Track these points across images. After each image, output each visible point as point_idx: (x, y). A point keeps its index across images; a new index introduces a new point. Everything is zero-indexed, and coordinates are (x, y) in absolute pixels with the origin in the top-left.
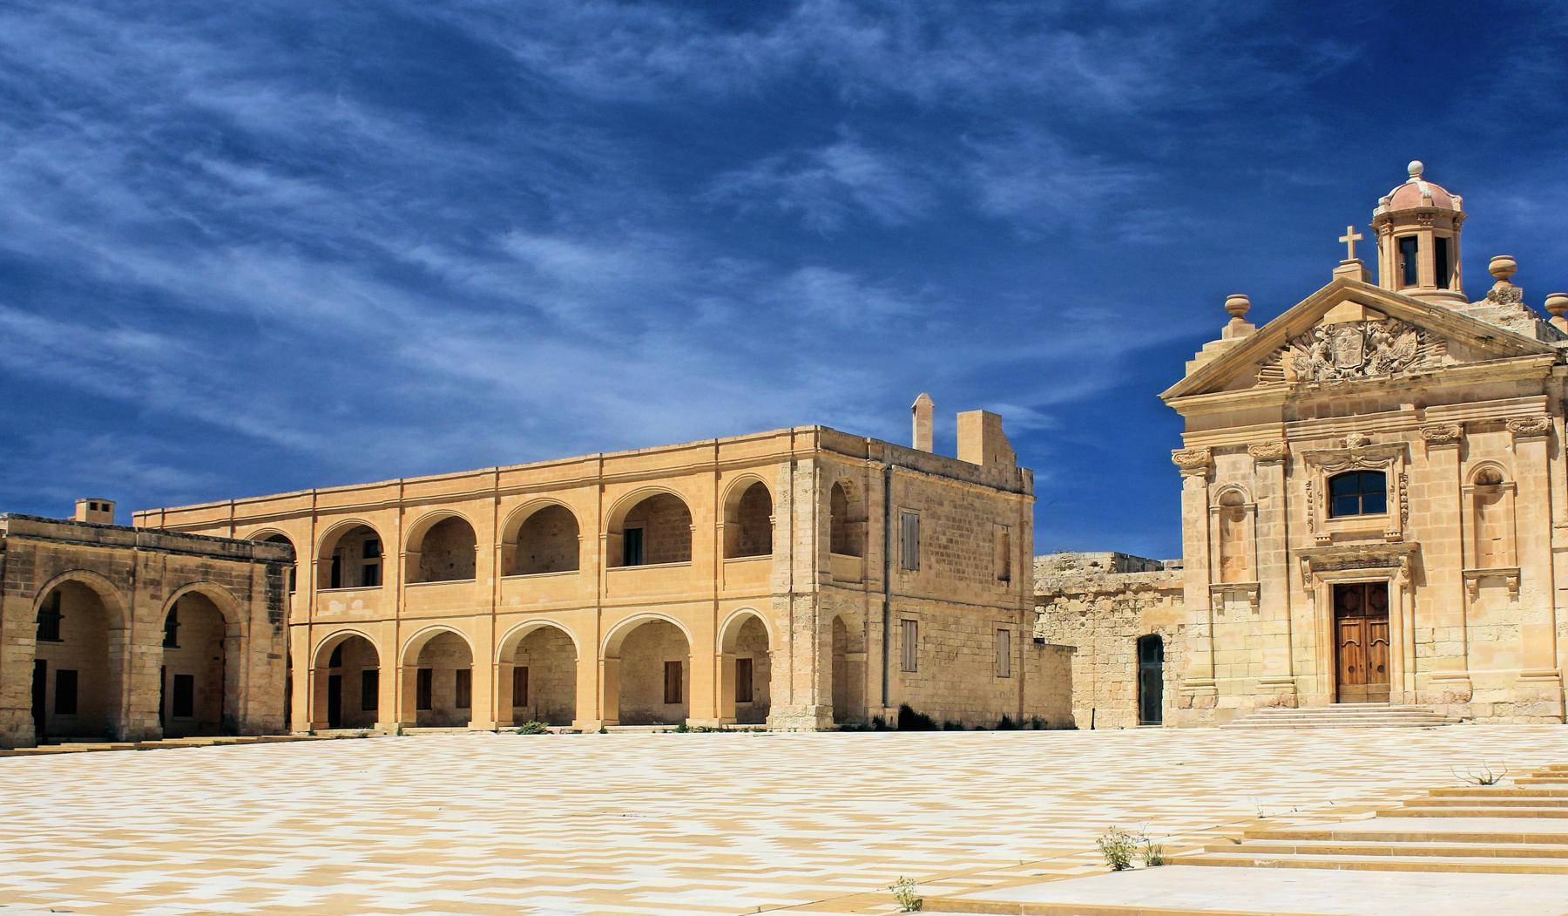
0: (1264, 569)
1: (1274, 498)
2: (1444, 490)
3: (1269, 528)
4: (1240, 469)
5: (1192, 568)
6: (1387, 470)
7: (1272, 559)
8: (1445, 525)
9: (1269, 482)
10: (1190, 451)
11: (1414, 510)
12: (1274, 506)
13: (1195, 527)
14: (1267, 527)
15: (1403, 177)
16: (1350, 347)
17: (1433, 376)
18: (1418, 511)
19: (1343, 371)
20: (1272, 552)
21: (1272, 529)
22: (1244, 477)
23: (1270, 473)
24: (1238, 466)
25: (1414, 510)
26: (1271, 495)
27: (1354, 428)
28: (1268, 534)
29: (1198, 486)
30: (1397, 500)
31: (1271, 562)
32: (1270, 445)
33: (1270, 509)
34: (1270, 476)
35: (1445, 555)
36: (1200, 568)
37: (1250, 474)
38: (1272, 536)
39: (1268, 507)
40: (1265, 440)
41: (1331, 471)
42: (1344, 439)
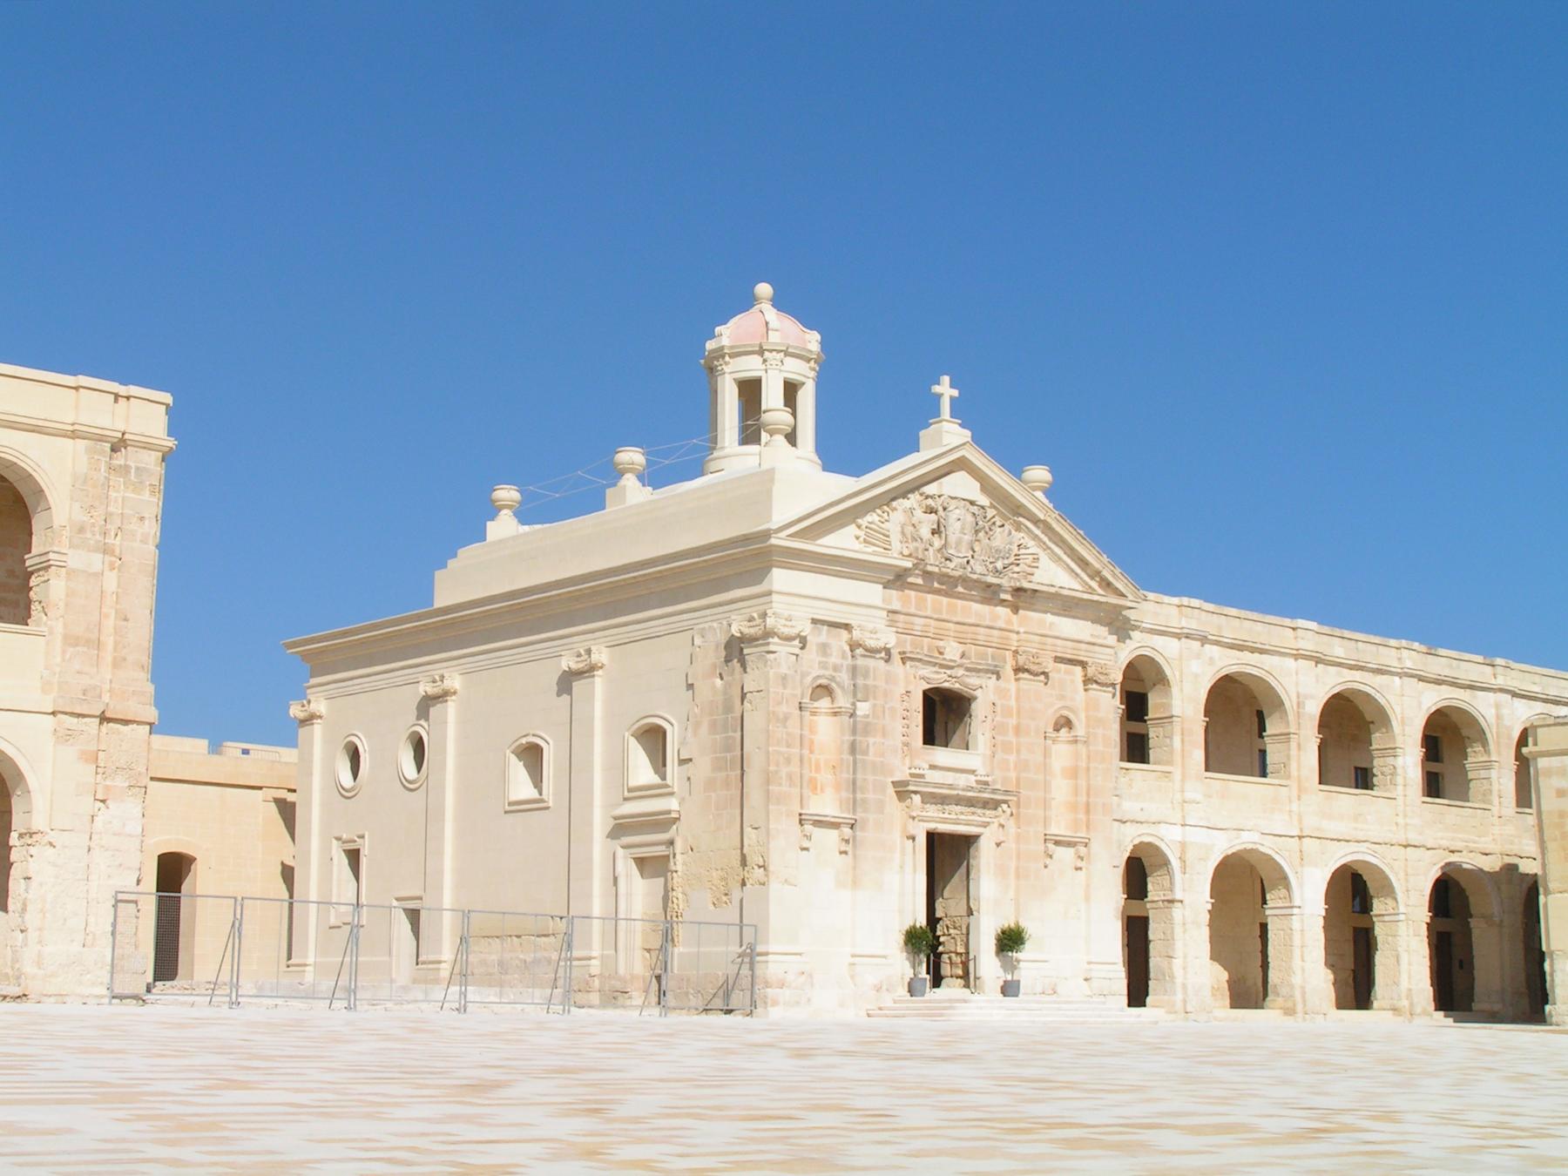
0: (862, 800)
3: (868, 745)
4: (831, 655)
5: (780, 785)
6: (978, 693)
10: (790, 616)
13: (785, 727)
15: (747, 302)
17: (1038, 594)
21: (871, 745)
22: (836, 668)
23: (872, 670)
24: (829, 651)
27: (952, 634)
28: (866, 753)
29: (789, 668)
30: (988, 735)
32: (876, 633)
33: (870, 720)
35: (1030, 811)
36: (790, 786)
37: (842, 666)
39: (868, 716)
42: (941, 643)
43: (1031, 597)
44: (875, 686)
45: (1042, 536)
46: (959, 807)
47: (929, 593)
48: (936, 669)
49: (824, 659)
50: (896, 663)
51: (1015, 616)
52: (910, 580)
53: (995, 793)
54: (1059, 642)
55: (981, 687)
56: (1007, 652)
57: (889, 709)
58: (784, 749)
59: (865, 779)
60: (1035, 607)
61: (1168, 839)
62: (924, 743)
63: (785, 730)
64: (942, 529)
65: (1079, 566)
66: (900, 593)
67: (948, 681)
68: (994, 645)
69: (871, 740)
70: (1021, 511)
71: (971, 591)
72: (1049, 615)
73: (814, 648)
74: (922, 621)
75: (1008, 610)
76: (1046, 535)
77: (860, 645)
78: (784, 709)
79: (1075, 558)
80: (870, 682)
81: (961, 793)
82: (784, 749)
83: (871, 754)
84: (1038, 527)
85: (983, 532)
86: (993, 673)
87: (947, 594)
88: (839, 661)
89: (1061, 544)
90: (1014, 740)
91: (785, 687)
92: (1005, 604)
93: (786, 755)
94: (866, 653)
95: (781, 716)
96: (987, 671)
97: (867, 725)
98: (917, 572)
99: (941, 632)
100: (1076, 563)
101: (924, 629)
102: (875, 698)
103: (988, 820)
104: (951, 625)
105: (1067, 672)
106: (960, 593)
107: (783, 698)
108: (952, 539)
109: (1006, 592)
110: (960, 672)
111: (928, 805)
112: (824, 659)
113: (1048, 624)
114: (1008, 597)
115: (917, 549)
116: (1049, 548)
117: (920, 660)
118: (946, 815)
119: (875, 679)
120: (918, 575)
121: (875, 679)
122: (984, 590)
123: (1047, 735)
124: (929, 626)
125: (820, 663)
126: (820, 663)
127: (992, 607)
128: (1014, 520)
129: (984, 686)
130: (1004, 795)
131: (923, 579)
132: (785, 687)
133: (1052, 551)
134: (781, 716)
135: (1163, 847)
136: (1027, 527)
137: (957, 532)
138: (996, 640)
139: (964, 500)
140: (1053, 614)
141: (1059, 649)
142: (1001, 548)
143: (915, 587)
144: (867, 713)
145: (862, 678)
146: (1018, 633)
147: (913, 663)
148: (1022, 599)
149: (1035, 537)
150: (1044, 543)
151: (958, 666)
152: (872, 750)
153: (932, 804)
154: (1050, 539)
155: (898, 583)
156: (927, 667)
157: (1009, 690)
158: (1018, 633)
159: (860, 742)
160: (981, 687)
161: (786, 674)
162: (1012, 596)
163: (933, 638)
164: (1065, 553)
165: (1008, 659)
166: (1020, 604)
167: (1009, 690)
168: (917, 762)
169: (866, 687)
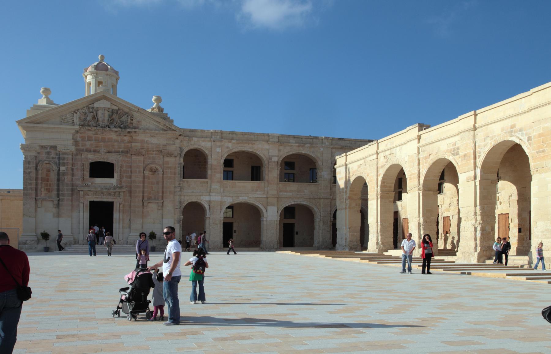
0: (62, 193)
1: (67, 167)
3: (65, 179)
4: (51, 155)
8: (137, 184)
9: (65, 161)
11: (125, 178)
17: (137, 132)
19: (101, 125)
20: (65, 187)
22: (53, 158)
23: (66, 158)
24: (50, 154)
25: (125, 178)
33: (66, 171)
34: (66, 160)
36: (31, 191)
37: (56, 157)
39: (65, 171)
44: (68, 162)
49: (48, 156)
58: (29, 181)
59: (63, 188)
61: (204, 200)
62: (90, 177)
63: (29, 176)
64: (96, 116)
69: (66, 177)
73: (44, 153)
78: (29, 170)
80: (65, 161)
82: (29, 181)
88: (55, 156)
91: (29, 164)
93: (30, 183)
95: (28, 172)
102: (67, 166)
105: (155, 154)
107: (28, 167)
108: (100, 119)
112: (48, 156)
113: (145, 141)
115: (84, 123)
119: (67, 160)
121: (67, 160)
125: (46, 157)
126: (46, 157)
132: (29, 164)
134: (28, 172)
135: (202, 202)
144: (64, 170)
152: (66, 180)
159: (61, 178)
161: (30, 161)
169: (63, 163)
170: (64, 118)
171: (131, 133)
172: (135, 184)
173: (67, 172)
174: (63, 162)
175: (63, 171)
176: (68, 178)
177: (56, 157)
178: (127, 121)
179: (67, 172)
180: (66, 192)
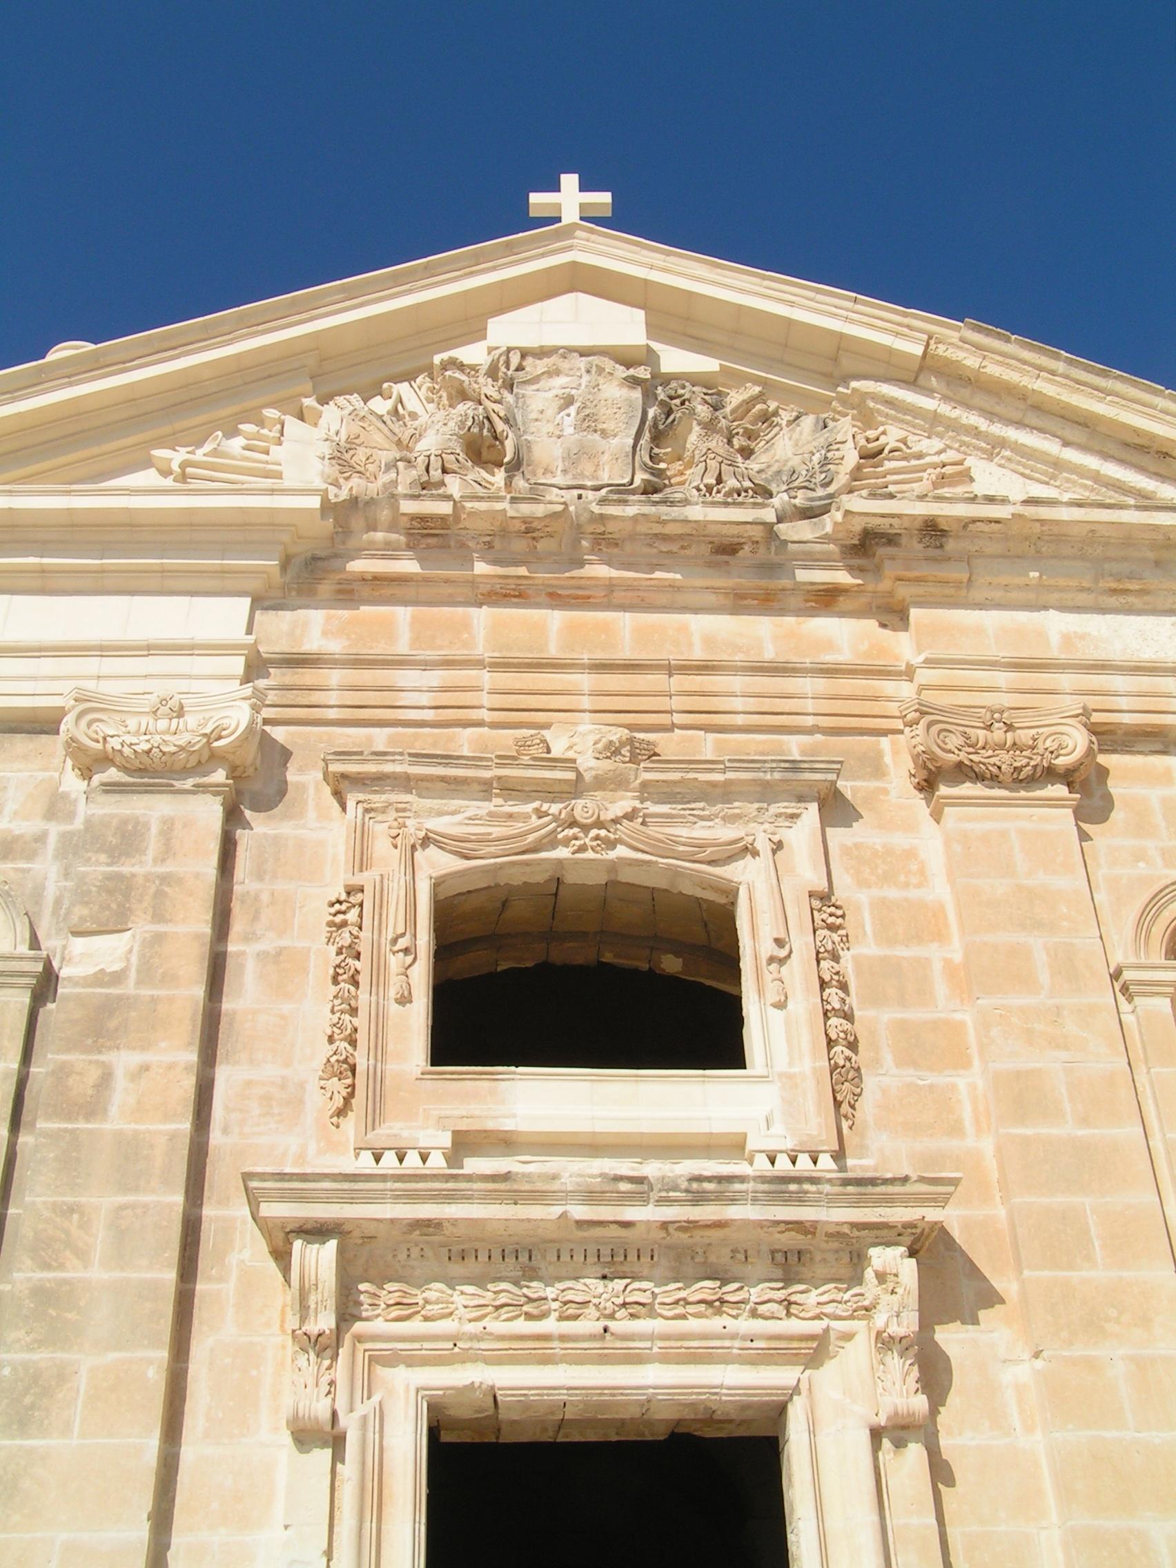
1: (159, 938)
2: (1044, 978)
3: (106, 1079)
6: (745, 874)
7: (99, 1238)
8: (1067, 1129)
9: (140, 867)
11: (888, 1058)
12: (147, 974)
14: (94, 1075)
16: (588, 422)
18: (907, 1059)
21: (120, 1082)
23: (154, 830)
25: (888, 1058)
26: (142, 927)
27: (586, 702)
28: (94, 1107)
30: (804, 1003)
31: (83, 1255)
33: (129, 987)
34: (153, 845)
37: (41, 838)
38: (116, 1121)
39: (118, 978)
40: (160, 688)
41: (467, 858)
43: (934, 560)
44: (165, 879)
45: (945, 409)
46: (619, 1284)
47: (480, 605)
48: (497, 804)
50: (311, 814)
51: (902, 635)
52: (358, 566)
53: (800, 1199)
54: (1119, 682)
55: (755, 854)
56: (885, 742)
57: (262, 956)
60: (977, 595)
65: (1141, 469)
66: (345, 614)
67: (566, 842)
68: (810, 721)
69: (123, 1060)
70: (847, 364)
71: (653, 567)
72: (1052, 613)
74: (436, 677)
75: (871, 624)
76: (968, 407)
77: (105, 760)
79: (1112, 448)
80: (140, 867)
81: (580, 1212)
83: (114, 1110)
84: (929, 392)
85: (697, 429)
86: (801, 799)
87: (556, 599)
89: (1033, 419)
90: (966, 1017)
92: (843, 603)
94: (127, 779)
96: (765, 793)
97: (109, 1007)
98: (379, 536)
99: (533, 701)
100: (1121, 462)
101: (446, 698)
102: (158, 917)
103: (817, 1327)
104: (585, 681)
106: (611, 586)
109: (811, 560)
110: (623, 804)
111: (436, 1290)
114: (842, 577)
116: (1002, 443)
117: (405, 783)
118: (550, 1325)
120: (388, 545)
122: (711, 565)
123: (1127, 975)
124: (479, 689)
127: (790, 620)
128: (843, 400)
129: (763, 845)
130: (858, 1202)
131: (421, 560)
133: (1018, 449)
136: (890, 402)
137: (569, 430)
138: (810, 706)
139: (584, 352)
140: (1063, 608)
141: (1123, 703)
142: (795, 462)
143: (397, 591)
144: (116, 967)
145: (103, 857)
146: (908, 673)
147: (378, 799)
148: (890, 570)
149: (934, 423)
150: (976, 432)
151: (601, 783)
152: (122, 1094)
153: (451, 1283)
154: (991, 416)
155: (326, 589)
156: (456, 803)
157: (910, 854)
158: (908, 673)
160: (755, 854)
162: (850, 569)
163: (494, 725)
164: (1066, 444)
165: (888, 759)
166: (903, 591)
167: (910, 854)
168: (393, 1129)
170: (184, 465)
171: (882, 551)
172: (1044, 1131)
173: (146, 992)
174: (119, 877)
175: (100, 979)
176: (145, 1068)
177: (41, 838)
178: (825, 462)
179: (146, 992)
180: (97, 1273)
